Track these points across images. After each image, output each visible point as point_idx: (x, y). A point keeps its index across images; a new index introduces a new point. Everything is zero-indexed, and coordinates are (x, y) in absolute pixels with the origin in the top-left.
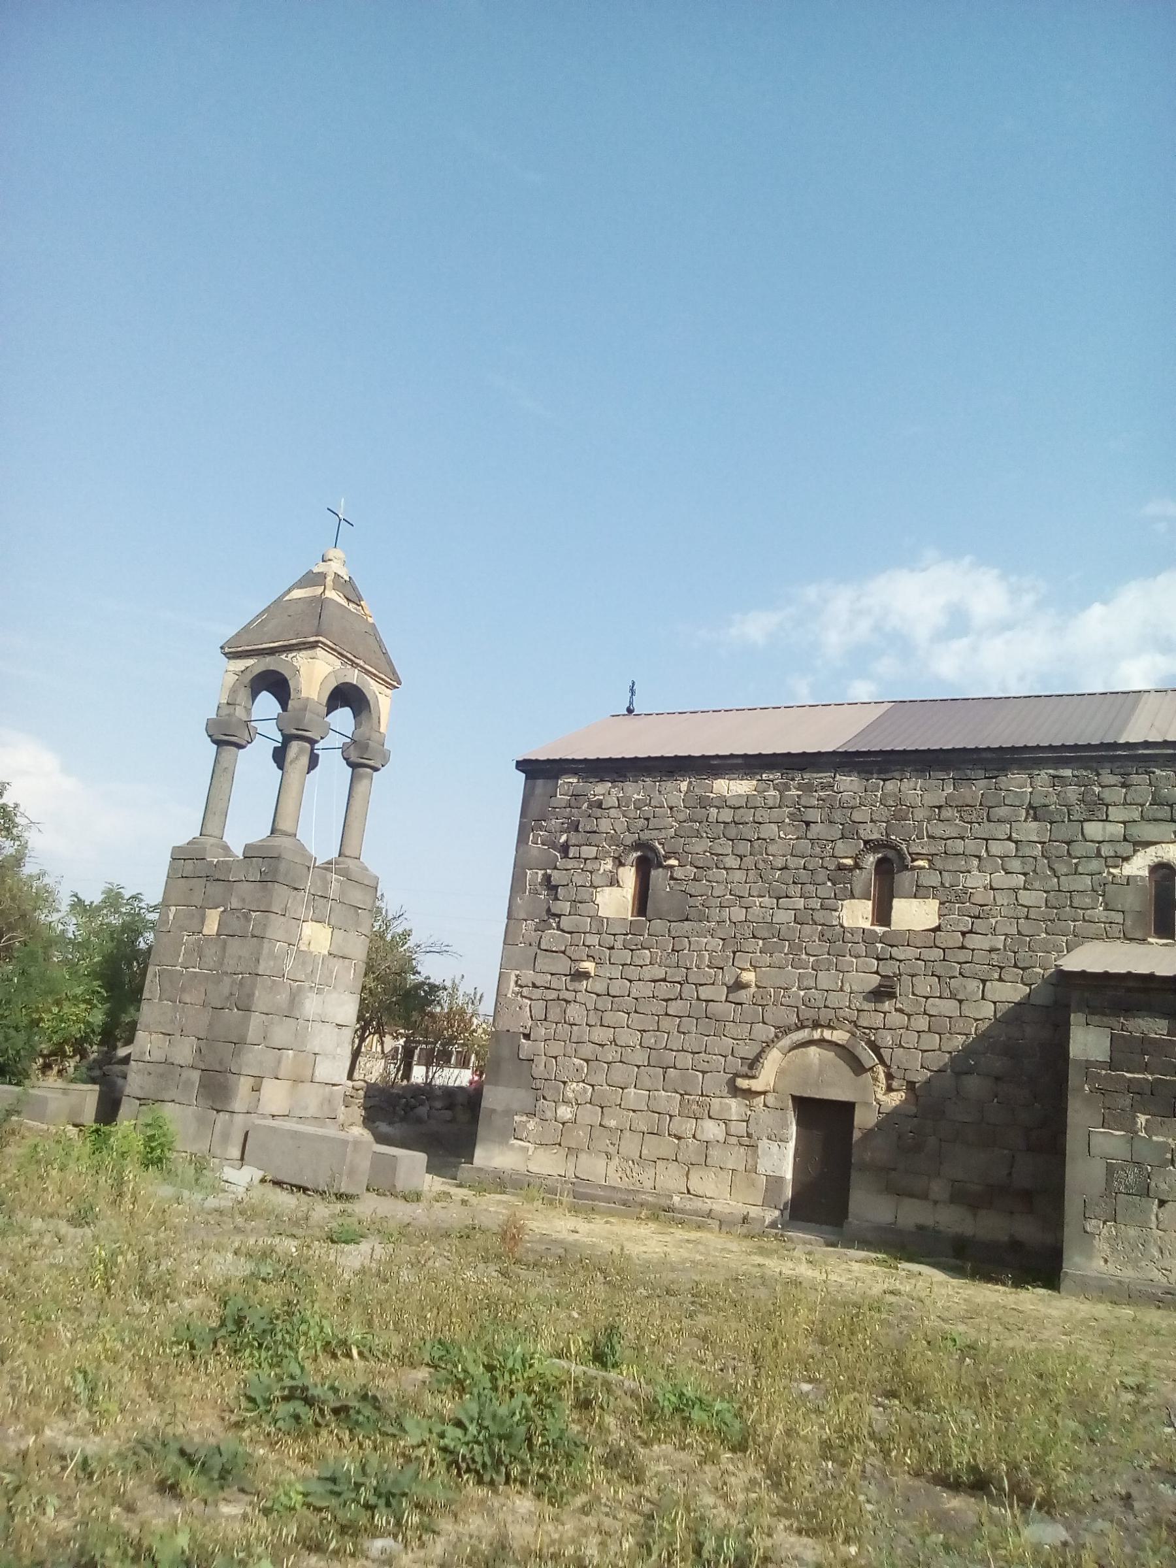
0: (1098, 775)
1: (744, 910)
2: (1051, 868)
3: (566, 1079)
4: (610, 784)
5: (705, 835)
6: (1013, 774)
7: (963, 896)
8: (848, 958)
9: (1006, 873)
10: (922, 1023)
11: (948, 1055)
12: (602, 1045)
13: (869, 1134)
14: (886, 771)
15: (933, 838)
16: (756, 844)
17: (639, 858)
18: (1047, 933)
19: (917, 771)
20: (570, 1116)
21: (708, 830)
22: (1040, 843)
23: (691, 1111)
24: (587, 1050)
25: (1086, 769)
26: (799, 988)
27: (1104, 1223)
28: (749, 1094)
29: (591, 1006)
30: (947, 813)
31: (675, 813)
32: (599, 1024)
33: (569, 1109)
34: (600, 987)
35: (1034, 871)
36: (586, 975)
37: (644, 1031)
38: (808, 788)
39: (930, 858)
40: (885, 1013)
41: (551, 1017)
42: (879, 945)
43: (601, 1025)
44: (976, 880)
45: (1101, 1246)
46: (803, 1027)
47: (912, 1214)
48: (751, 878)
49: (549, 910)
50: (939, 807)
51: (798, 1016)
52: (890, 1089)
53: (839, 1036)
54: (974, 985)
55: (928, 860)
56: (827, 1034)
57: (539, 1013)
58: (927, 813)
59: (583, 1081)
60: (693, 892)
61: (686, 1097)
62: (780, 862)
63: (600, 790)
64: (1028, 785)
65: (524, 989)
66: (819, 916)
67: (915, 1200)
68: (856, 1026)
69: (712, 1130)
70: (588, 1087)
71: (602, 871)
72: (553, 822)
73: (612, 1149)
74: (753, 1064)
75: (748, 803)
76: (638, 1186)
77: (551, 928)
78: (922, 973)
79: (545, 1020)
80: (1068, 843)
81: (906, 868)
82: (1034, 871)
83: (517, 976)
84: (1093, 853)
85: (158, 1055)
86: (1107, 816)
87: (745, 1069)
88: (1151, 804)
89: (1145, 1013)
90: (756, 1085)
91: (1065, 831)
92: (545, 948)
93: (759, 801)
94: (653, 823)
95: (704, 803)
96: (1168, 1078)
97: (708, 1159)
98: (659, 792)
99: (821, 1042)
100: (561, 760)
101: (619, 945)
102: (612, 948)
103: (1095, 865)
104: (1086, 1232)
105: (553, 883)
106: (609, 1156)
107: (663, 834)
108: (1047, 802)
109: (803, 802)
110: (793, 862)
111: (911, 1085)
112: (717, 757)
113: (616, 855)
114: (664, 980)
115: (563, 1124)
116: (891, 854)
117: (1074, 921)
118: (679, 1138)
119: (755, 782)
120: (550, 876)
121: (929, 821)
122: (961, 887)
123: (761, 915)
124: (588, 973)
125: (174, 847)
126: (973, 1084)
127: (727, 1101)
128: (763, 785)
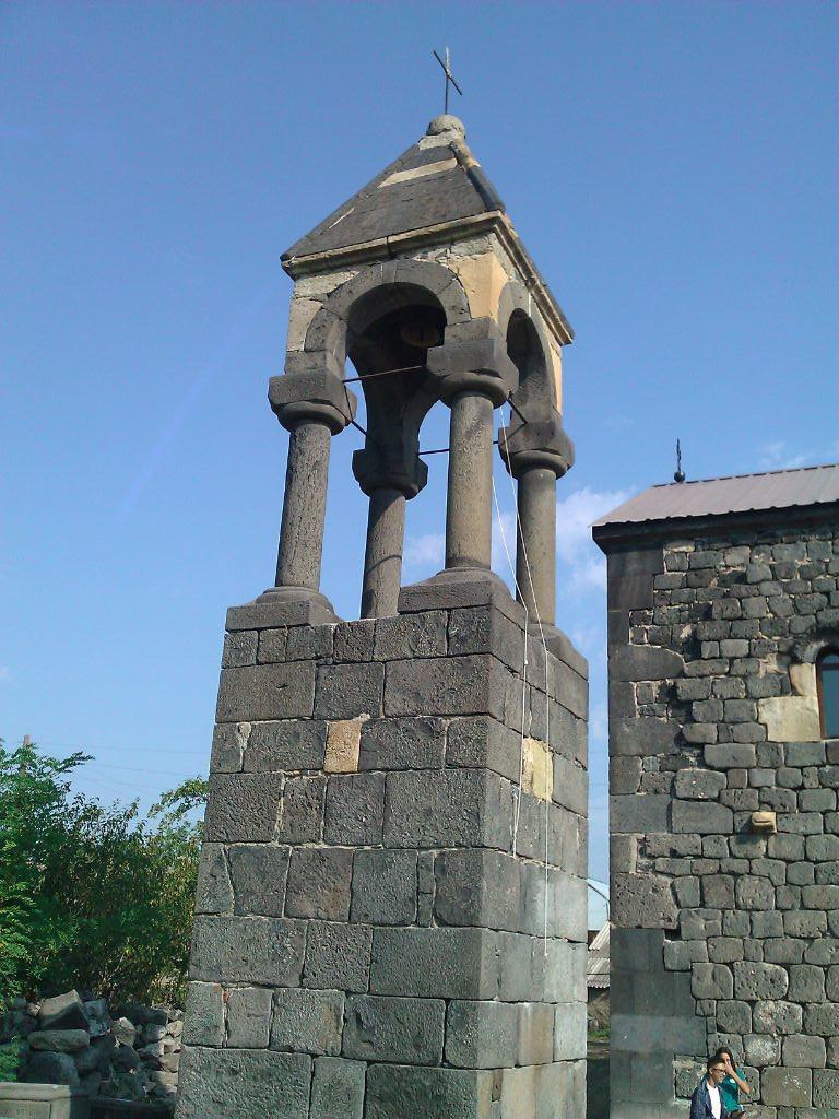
3: (754, 997)
12: (811, 940)
20: (770, 1055)
24: (784, 949)
29: (779, 880)
33: (768, 1045)
34: (791, 848)
36: (766, 832)
41: (712, 900)
43: (803, 907)
59: (785, 998)
63: (735, 558)
65: (659, 860)
71: (762, 673)
72: (665, 609)
77: (686, 764)
79: (701, 906)
85: (244, 1031)
92: (686, 795)
101: (811, 781)
102: (802, 787)
105: (683, 698)
113: (783, 648)
115: (760, 1068)
120: (675, 687)
124: (771, 827)
125: (230, 609)
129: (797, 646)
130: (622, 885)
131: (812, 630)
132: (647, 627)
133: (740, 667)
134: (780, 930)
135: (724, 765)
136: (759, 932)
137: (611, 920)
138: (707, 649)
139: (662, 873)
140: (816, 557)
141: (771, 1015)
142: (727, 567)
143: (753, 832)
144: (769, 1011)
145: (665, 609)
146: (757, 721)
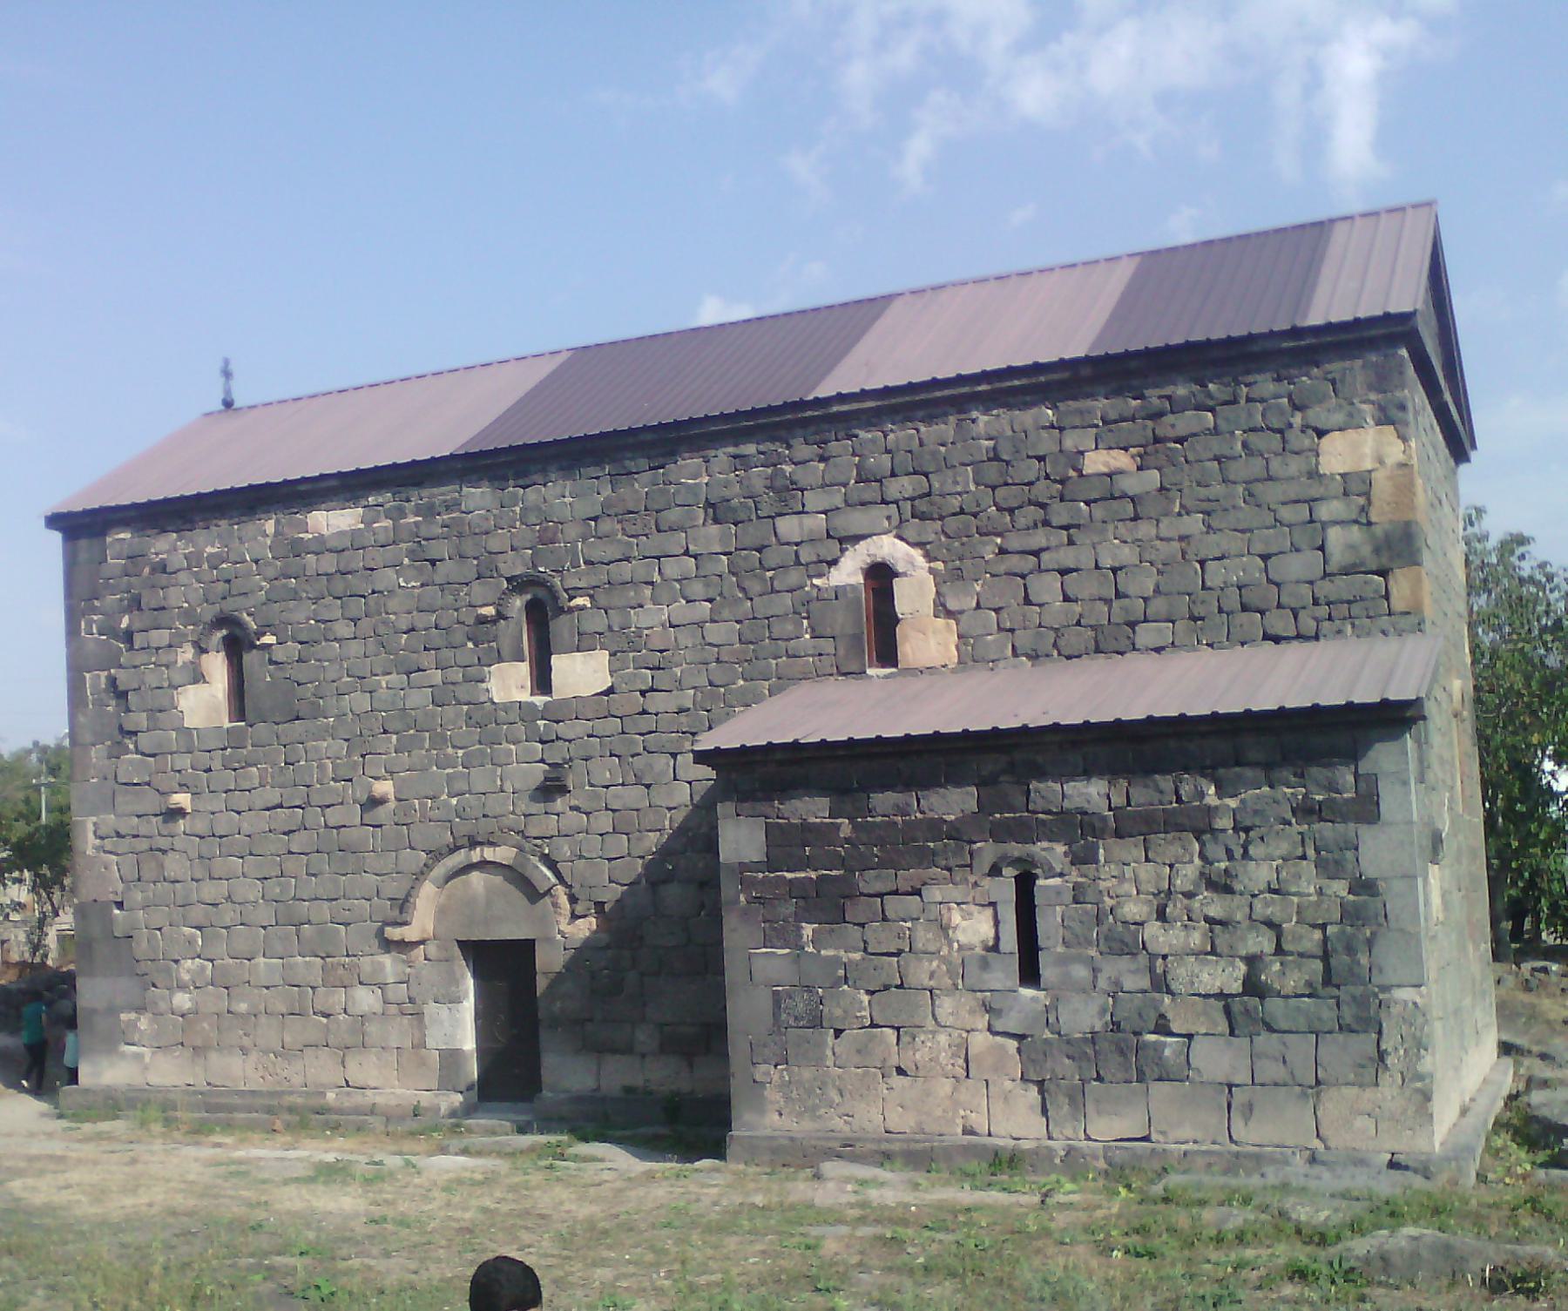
0: (789, 447)
1: (368, 694)
2: (743, 590)
3: (177, 957)
6: (684, 459)
8: (505, 745)
9: (687, 602)
10: (604, 821)
11: (640, 861)
15: (592, 563)
17: (224, 638)
18: (745, 680)
19: (562, 469)
22: (725, 554)
24: (197, 913)
25: (773, 440)
26: (451, 796)
28: (403, 946)
30: (606, 525)
34: (201, 826)
36: (179, 812)
37: (266, 878)
38: (429, 511)
41: (146, 875)
43: (211, 878)
44: (651, 617)
46: (458, 848)
49: (121, 728)
50: (595, 519)
51: (452, 833)
53: (502, 854)
54: (663, 762)
55: (591, 597)
56: (489, 854)
57: (131, 872)
59: (199, 957)
61: (328, 960)
63: (165, 546)
64: (704, 474)
69: (366, 999)
70: (206, 963)
71: (180, 663)
74: (403, 904)
77: (127, 751)
78: (597, 754)
79: (139, 880)
82: (721, 594)
84: (791, 559)
86: (803, 505)
88: (856, 482)
90: (409, 933)
91: (755, 532)
92: (124, 781)
94: (238, 585)
95: (297, 549)
97: (366, 1038)
98: (240, 539)
99: (483, 865)
102: (209, 770)
103: (794, 577)
105: (121, 688)
107: (249, 602)
108: (726, 493)
109: (424, 532)
111: (599, 905)
112: (304, 480)
114: (282, 807)
116: (541, 593)
117: (775, 659)
118: (327, 1016)
119: (360, 510)
122: (633, 629)
124: (182, 809)
126: (673, 894)
128: (371, 514)
134: (195, 897)
139: (111, 853)
141: (188, 971)
146: (176, 708)
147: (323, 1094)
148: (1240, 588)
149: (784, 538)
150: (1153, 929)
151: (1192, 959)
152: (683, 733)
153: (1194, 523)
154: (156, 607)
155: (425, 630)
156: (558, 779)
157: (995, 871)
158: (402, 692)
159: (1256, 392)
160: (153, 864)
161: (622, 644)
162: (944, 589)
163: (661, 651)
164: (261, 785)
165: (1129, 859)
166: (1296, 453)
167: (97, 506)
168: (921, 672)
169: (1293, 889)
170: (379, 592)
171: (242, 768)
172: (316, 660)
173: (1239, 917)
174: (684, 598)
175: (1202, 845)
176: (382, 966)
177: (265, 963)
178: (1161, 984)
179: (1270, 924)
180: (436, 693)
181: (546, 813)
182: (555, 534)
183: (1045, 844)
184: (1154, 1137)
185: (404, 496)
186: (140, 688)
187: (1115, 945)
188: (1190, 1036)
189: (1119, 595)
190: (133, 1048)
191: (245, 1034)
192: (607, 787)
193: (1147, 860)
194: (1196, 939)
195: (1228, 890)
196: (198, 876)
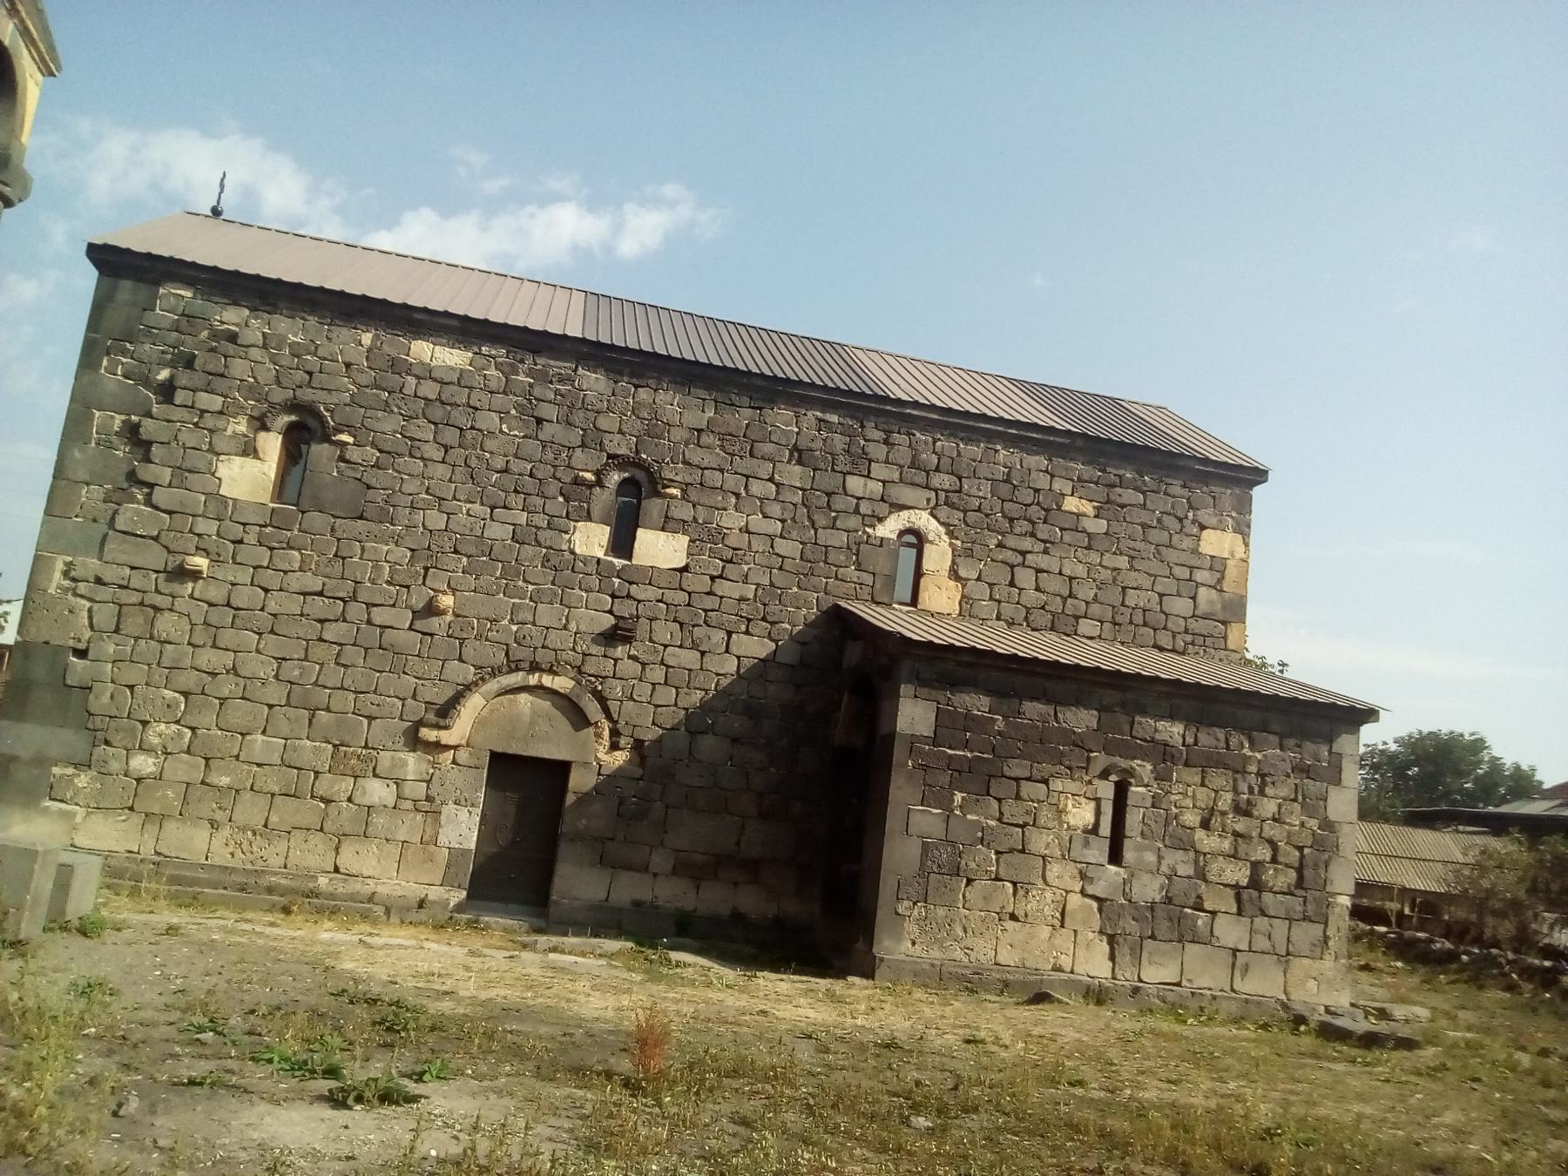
0: (862, 426)
1: (445, 515)
3: (148, 718)
4: (247, 312)
5: (396, 410)
6: (780, 409)
7: (720, 535)
8: (577, 591)
9: (764, 517)
11: (683, 712)
12: (214, 674)
13: (584, 798)
14: (639, 376)
15: (690, 464)
16: (469, 435)
18: (799, 587)
20: (152, 769)
21: (402, 404)
22: (801, 489)
23: (349, 767)
24: (189, 679)
25: (852, 417)
27: (915, 903)
28: (438, 747)
30: (707, 439)
31: (354, 374)
32: (211, 644)
33: (151, 761)
34: (216, 593)
35: (793, 519)
36: (195, 575)
38: (543, 377)
39: (685, 487)
40: (616, 660)
42: (617, 581)
43: (214, 646)
44: (732, 520)
45: (911, 928)
46: (517, 669)
47: (628, 889)
48: (458, 477)
50: (700, 431)
51: (507, 654)
52: (614, 747)
53: (562, 683)
55: (684, 491)
56: (547, 680)
58: (685, 434)
59: (178, 722)
60: (373, 482)
62: (499, 463)
63: (232, 317)
65: (81, 585)
66: (545, 536)
67: (631, 873)
68: (580, 672)
69: (378, 792)
71: (229, 432)
72: (147, 347)
73: (220, 816)
74: (445, 712)
75: (461, 379)
76: (259, 866)
77: (133, 500)
80: (829, 494)
81: (658, 494)
82: (793, 519)
83: (69, 565)
87: (431, 717)
89: (970, 689)
90: (446, 737)
91: (828, 481)
93: (478, 380)
95: (398, 366)
96: (985, 756)
97: (370, 829)
99: (539, 689)
100: (171, 259)
101: (251, 538)
102: (241, 542)
103: (853, 522)
104: (897, 914)
105: (144, 437)
106: (214, 824)
108: (813, 445)
109: (537, 391)
110: (516, 465)
112: (425, 310)
114: (320, 594)
115: (139, 780)
116: (640, 475)
118: (327, 801)
120: (137, 426)
121: (686, 444)
123: (469, 525)
124: (200, 572)
126: (709, 745)
127: (402, 755)
128: (481, 361)
129: (269, 414)
130: (38, 602)
131: (286, 404)
132: (124, 360)
133: (209, 421)
134: (187, 662)
135: (169, 508)
136: (166, 662)
137: (19, 633)
138: (181, 396)
139: (82, 596)
140: (309, 338)
141: (160, 735)
142: (223, 323)
143: (184, 574)
144: (158, 732)
145: (147, 347)
146: (213, 474)
147: (315, 878)
148: (1144, 611)
149: (850, 493)
150: (1200, 834)
151: (1221, 858)
152: (741, 617)
153: (1123, 562)
154: (213, 371)
155: (519, 475)
156: (630, 630)
157: (1104, 775)
158: (482, 522)
159: (1171, 490)
160: (141, 620)
161: (704, 537)
162: (958, 560)
163: (735, 549)
164: (301, 570)
165: (1189, 779)
166: (1187, 535)
167: (166, 254)
168: (932, 615)
169: (1288, 821)
170: (478, 430)
171: (283, 549)
172: (394, 470)
173: (1254, 834)
174: (762, 512)
175: (1235, 780)
176: (404, 764)
177: (263, 741)
178: (1201, 874)
179: (1272, 843)
180: (518, 530)
181: (605, 656)
182: (663, 432)
183: (1139, 762)
184: (1184, 983)
185: (519, 357)
186: (169, 443)
187: (1177, 842)
188: (1213, 913)
189: (1070, 596)
190: (63, 806)
191: (220, 808)
192: (666, 646)
193: (1203, 785)
194: (1226, 845)
195: (1247, 814)
196: (195, 641)
